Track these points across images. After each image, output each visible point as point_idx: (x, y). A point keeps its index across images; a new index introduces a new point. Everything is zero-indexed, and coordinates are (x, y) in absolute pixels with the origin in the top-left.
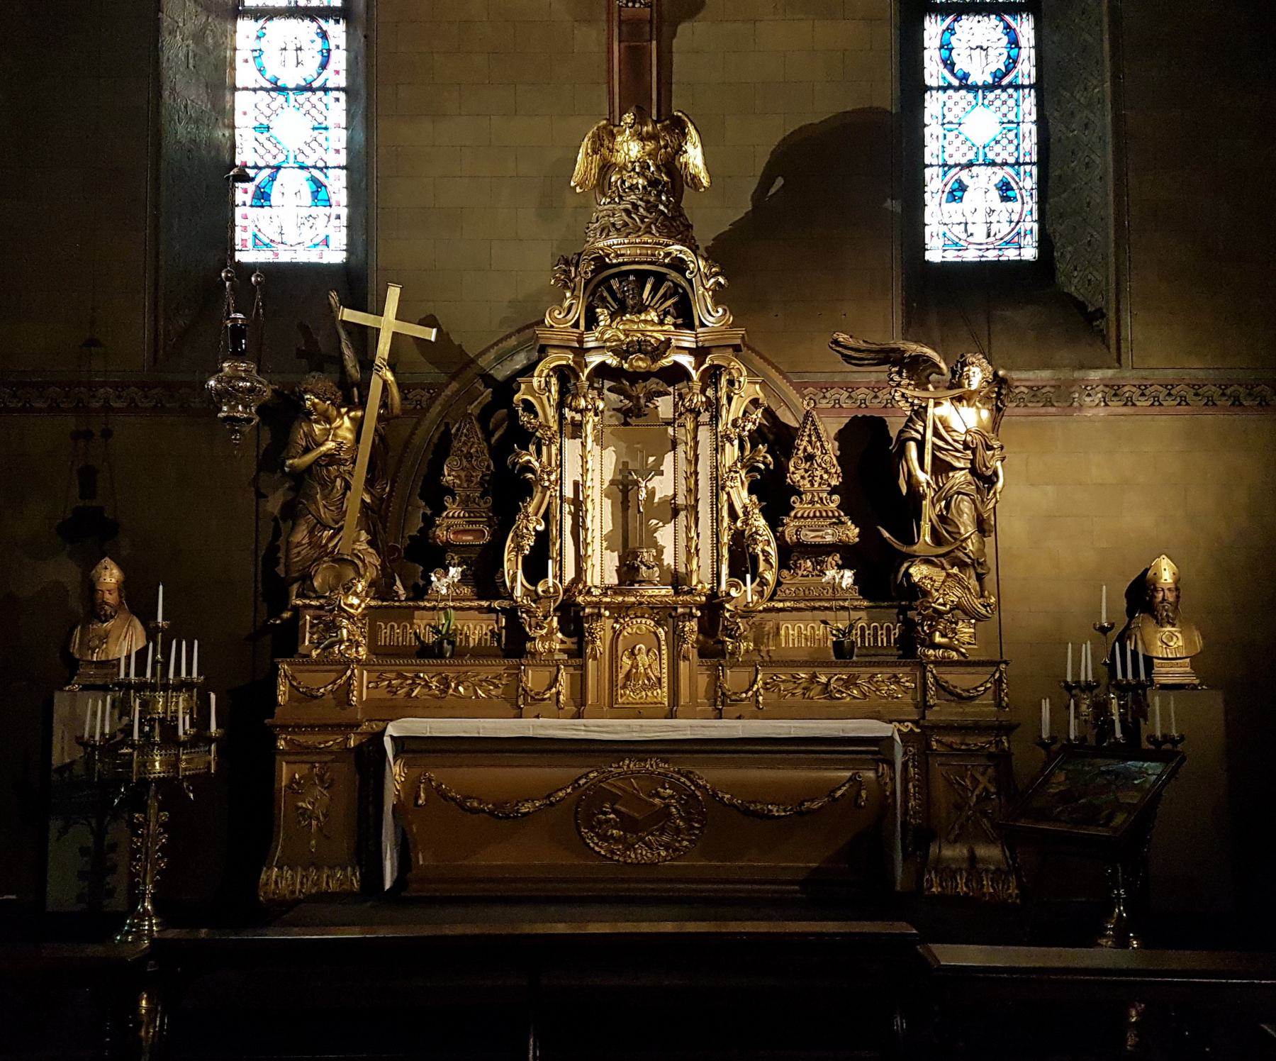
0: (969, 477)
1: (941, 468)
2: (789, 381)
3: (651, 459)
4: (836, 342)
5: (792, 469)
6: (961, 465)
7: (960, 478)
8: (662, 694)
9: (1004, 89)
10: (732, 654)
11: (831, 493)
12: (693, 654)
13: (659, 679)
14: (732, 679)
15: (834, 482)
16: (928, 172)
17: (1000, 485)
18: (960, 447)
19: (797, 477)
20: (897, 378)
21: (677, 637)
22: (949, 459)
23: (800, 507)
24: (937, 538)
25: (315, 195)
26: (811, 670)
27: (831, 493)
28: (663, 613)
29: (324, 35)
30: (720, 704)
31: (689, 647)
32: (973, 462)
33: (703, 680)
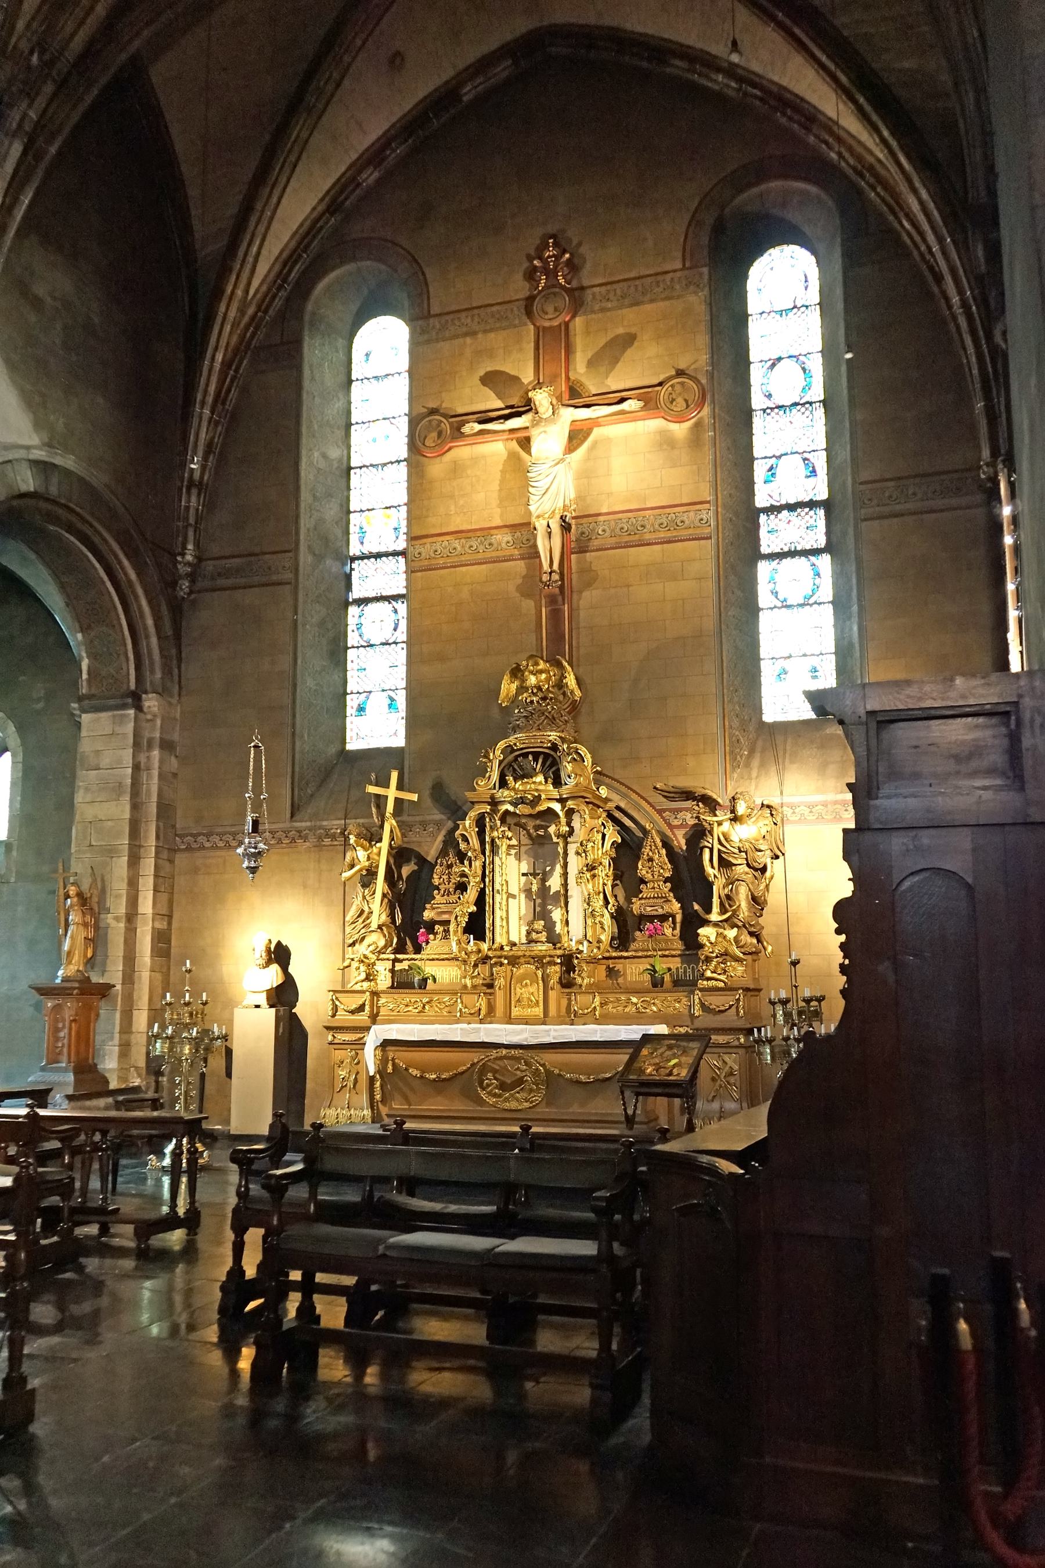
0: (747, 869)
1: (725, 864)
2: (654, 807)
3: (548, 868)
4: (655, 788)
5: (640, 867)
6: (739, 861)
7: (742, 869)
8: (539, 1011)
9: (811, 605)
10: (581, 986)
11: (665, 882)
12: (558, 987)
13: (537, 1001)
14: (580, 1001)
15: (668, 874)
16: (762, 662)
17: (768, 874)
18: (736, 851)
19: (644, 872)
20: (696, 808)
21: (545, 979)
22: (731, 859)
23: (646, 891)
24: (723, 910)
25: (390, 706)
26: (628, 995)
27: (665, 882)
28: (539, 961)
29: (396, 611)
30: (571, 1017)
31: (554, 981)
32: (747, 859)
33: (564, 1002)
